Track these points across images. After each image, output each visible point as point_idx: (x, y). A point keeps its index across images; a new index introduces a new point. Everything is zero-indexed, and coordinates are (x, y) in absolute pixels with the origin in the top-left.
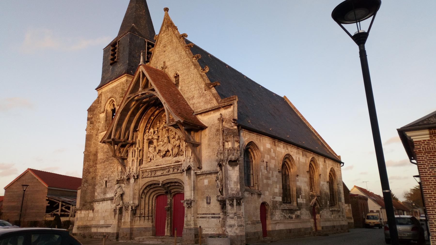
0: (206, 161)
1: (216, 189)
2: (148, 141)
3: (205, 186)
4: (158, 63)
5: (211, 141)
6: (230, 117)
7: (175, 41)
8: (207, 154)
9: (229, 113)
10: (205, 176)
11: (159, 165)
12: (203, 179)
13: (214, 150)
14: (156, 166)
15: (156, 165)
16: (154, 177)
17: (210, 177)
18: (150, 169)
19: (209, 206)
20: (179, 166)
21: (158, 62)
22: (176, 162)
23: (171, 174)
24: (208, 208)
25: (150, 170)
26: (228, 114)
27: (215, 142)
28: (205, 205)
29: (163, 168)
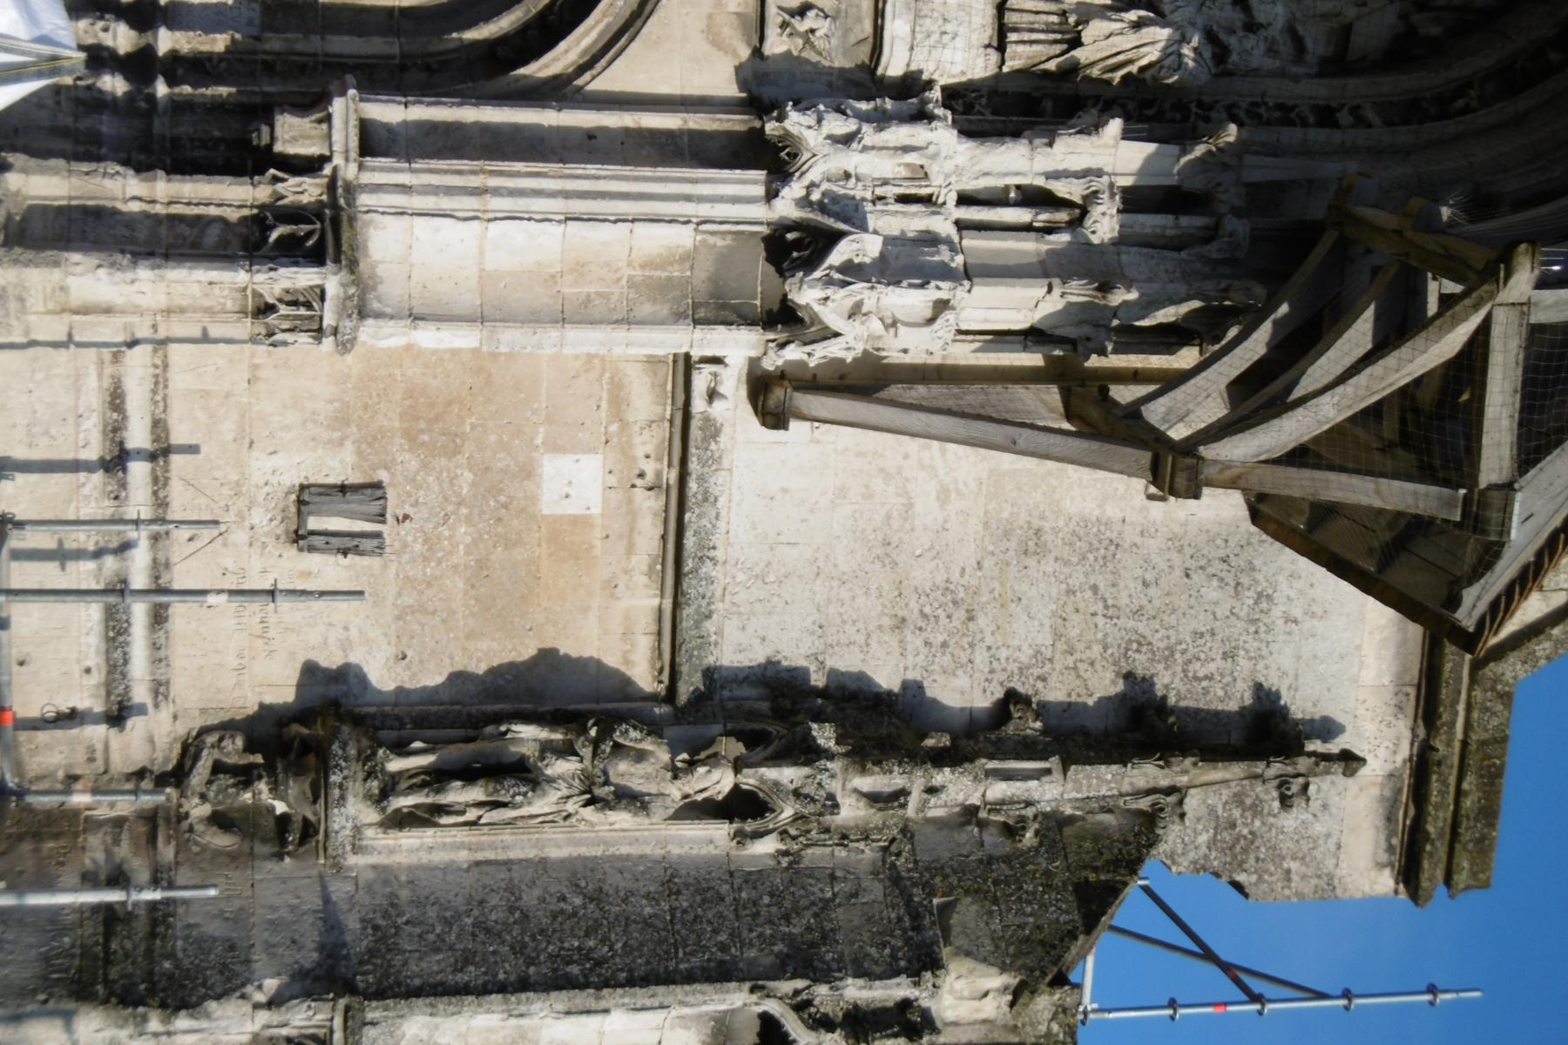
1: (469, 636)
3: (528, 472)
5: (1075, 582)
8: (927, 509)
9: (1333, 840)
10: (650, 468)
12: (624, 425)
17: (630, 550)
19: (259, 517)
24: (242, 503)
27: (1045, 638)
28: (276, 461)
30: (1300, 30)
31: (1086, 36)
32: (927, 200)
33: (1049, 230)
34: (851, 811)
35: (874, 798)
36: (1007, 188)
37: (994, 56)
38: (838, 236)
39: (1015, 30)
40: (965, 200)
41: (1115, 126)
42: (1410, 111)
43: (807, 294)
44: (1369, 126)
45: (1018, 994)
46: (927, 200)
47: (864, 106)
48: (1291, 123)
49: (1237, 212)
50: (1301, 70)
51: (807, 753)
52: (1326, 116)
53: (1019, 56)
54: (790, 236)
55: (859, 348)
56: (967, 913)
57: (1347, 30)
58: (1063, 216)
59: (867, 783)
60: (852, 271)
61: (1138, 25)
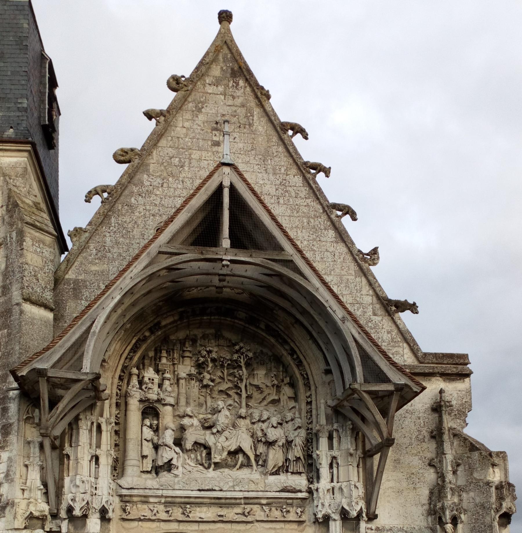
0: (389, 502)
2: (141, 406)
4: (186, 168)
6: (462, 405)
7: (260, 129)
11: (215, 490)
13: (412, 476)
14: (199, 490)
15: (200, 488)
16: (182, 524)
18: (166, 497)
20: (291, 501)
21: (187, 164)
22: (284, 490)
23: (258, 521)
25: (163, 500)
26: (456, 396)
29: (223, 501)
30: (290, 408)
31: (298, 456)
32: (333, 488)
33: (338, 464)
34: (456, 500)
35: (453, 495)
36: (330, 472)
37: (302, 475)
38: (343, 508)
39: (297, 470)
40: (332, 481)
41: (318, 452)
42: (307, 386)
43: (354, 514)
44: (311, 395)
45: (494, 465)
46: (333, 488)
47: (315, 502)
48: (311, 411)
49: (332, 427)
50: (297, 407)
51: (443, 509)
52: (309, 403)
53: (301, 469)
54: (343, 516)
55: (362, 501)
56: (476, 475)
57: (289, 397)
58: (334, 461)
59: (449, 496)
60: (350, 504)
61: (295, 445)
